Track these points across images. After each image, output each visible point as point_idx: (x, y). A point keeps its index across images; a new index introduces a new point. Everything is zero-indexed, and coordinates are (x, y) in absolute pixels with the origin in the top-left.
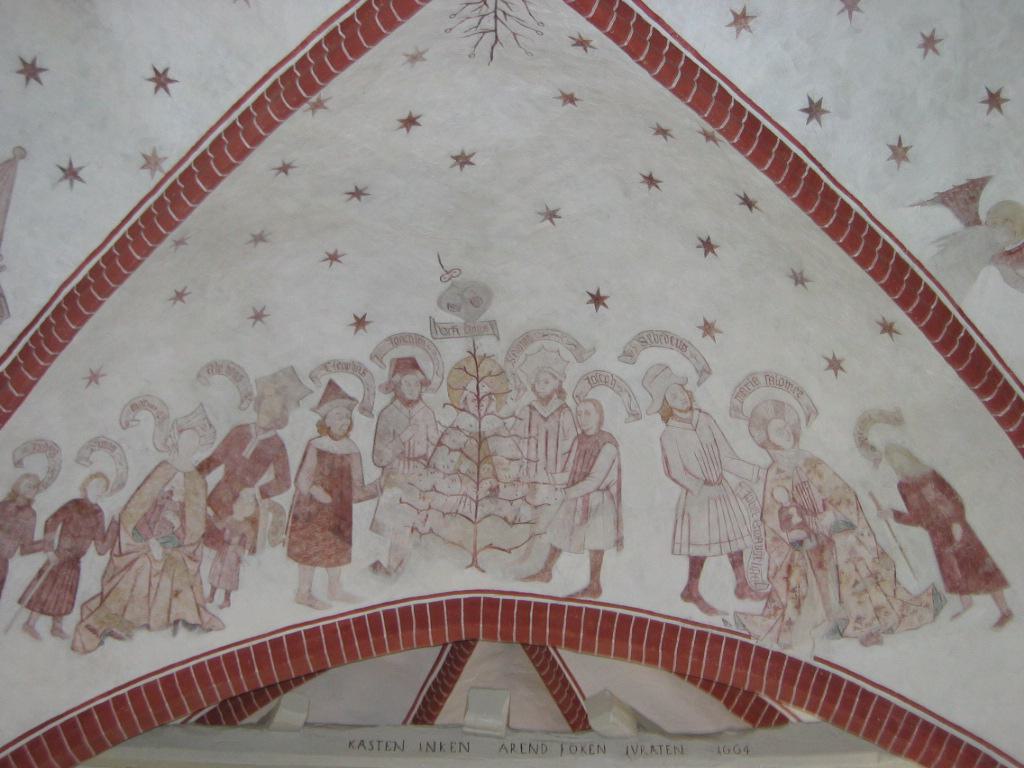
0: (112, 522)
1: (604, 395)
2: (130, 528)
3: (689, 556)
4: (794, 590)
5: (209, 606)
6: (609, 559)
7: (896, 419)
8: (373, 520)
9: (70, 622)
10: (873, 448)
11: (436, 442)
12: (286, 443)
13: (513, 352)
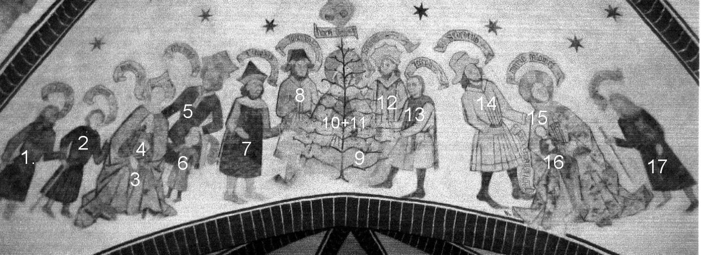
0: (106, 143)
1: (425, 73)
2: (118, 147)
3: (482, 172)
4: (551, 193)
5: (167, 200)
6: (430, 175)
7: (617, 75)
8: (276, 150)
9: (74, 207)
10: (601, 98)
11: (316, 103)
12: (221, 101)
13: (368, 45)
